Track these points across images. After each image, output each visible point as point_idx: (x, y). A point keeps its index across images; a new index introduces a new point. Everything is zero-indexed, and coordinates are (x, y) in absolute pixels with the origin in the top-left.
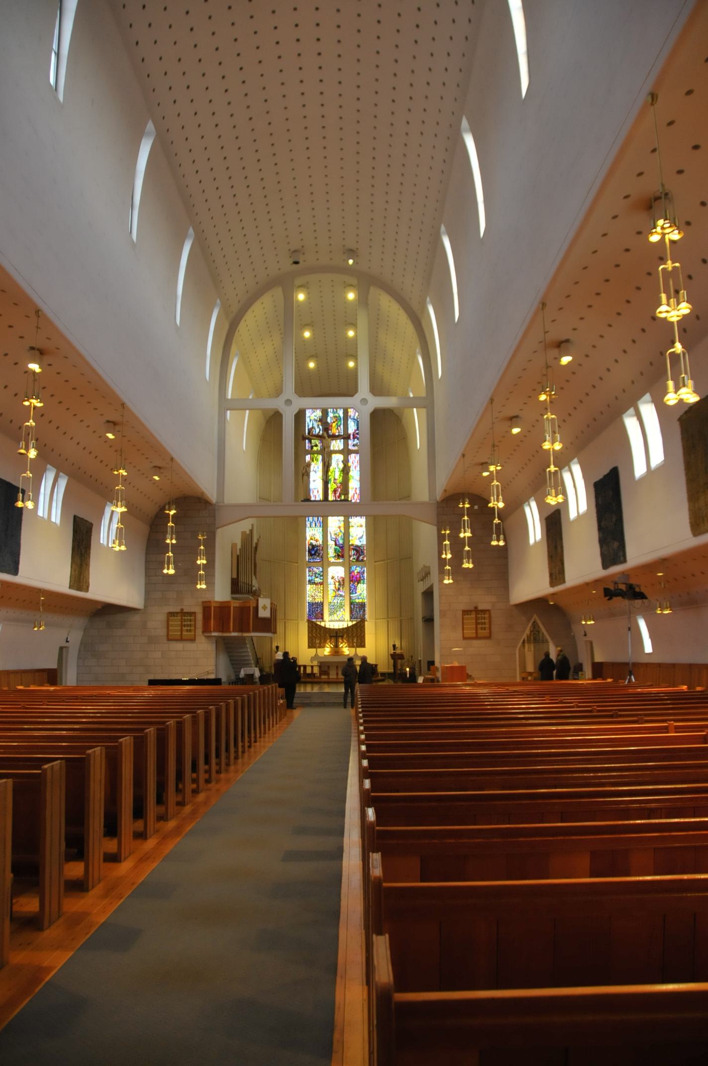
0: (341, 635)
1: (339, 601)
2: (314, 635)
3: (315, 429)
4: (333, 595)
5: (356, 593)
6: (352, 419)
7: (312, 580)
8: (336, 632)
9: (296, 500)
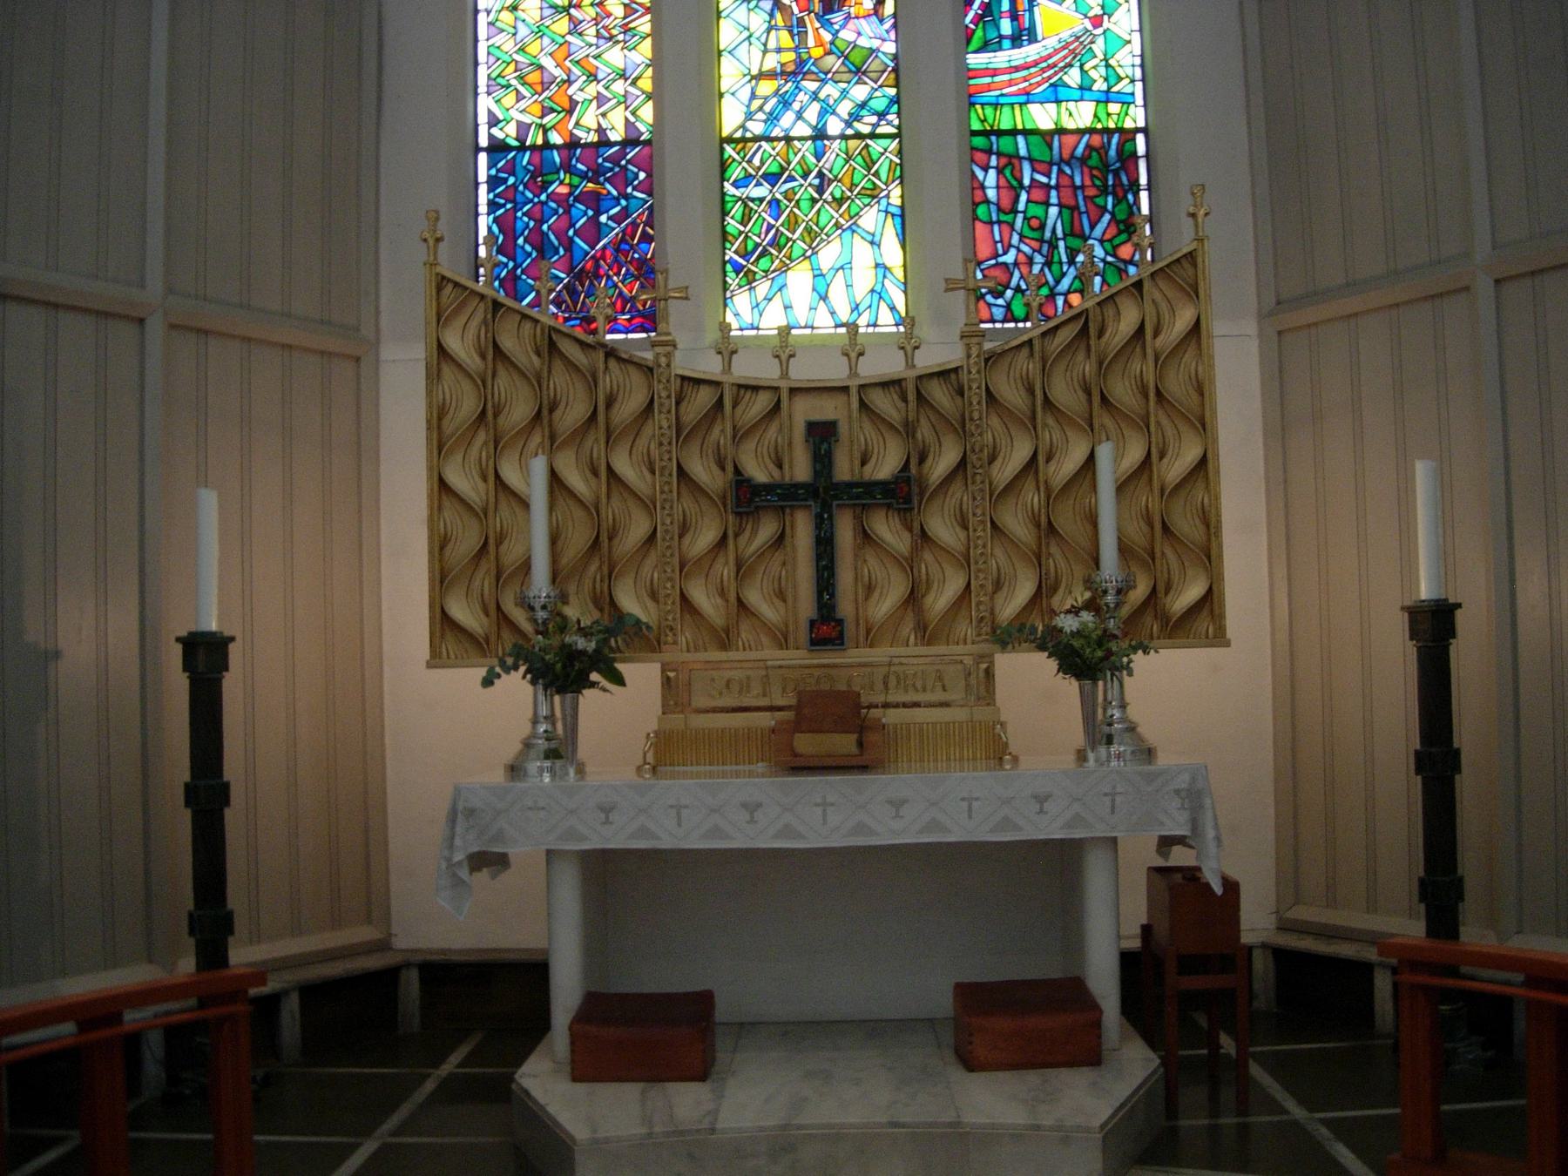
0: (885, 467)
1: (834, 127)
4: (771, 62)
5: (1024, 34)
8: (822, 434)
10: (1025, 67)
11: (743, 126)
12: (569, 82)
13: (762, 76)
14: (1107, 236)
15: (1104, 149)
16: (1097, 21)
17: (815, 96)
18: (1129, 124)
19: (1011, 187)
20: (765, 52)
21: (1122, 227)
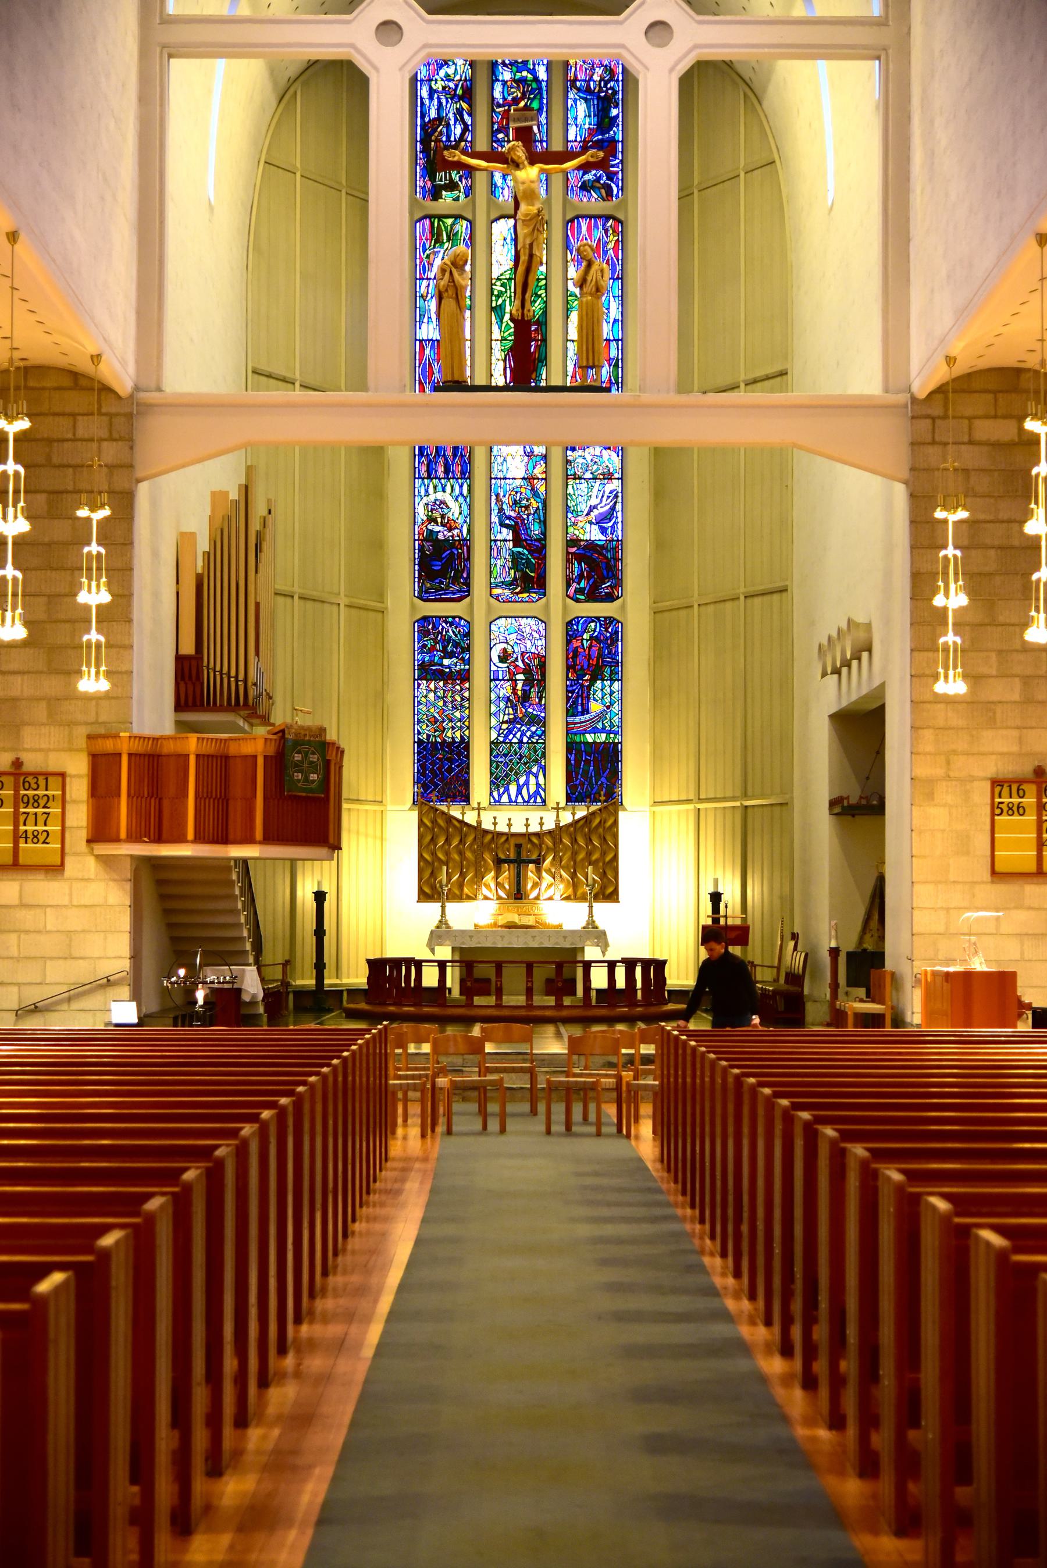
0: (534, 857)
1: (525, 740)
2: (441, 855)
3: (448, 125)
5: (586, 711)
6: (579, 90)
7: (432, 663)
8: (519, 847)
9: (683, 386)
10: (585, 722)
11: (497, 738)
12: (443, 722)
13: (503, 722)
16: (608, 707)
17: (519, 730)
18: (616, 741)
20: (504, 715)
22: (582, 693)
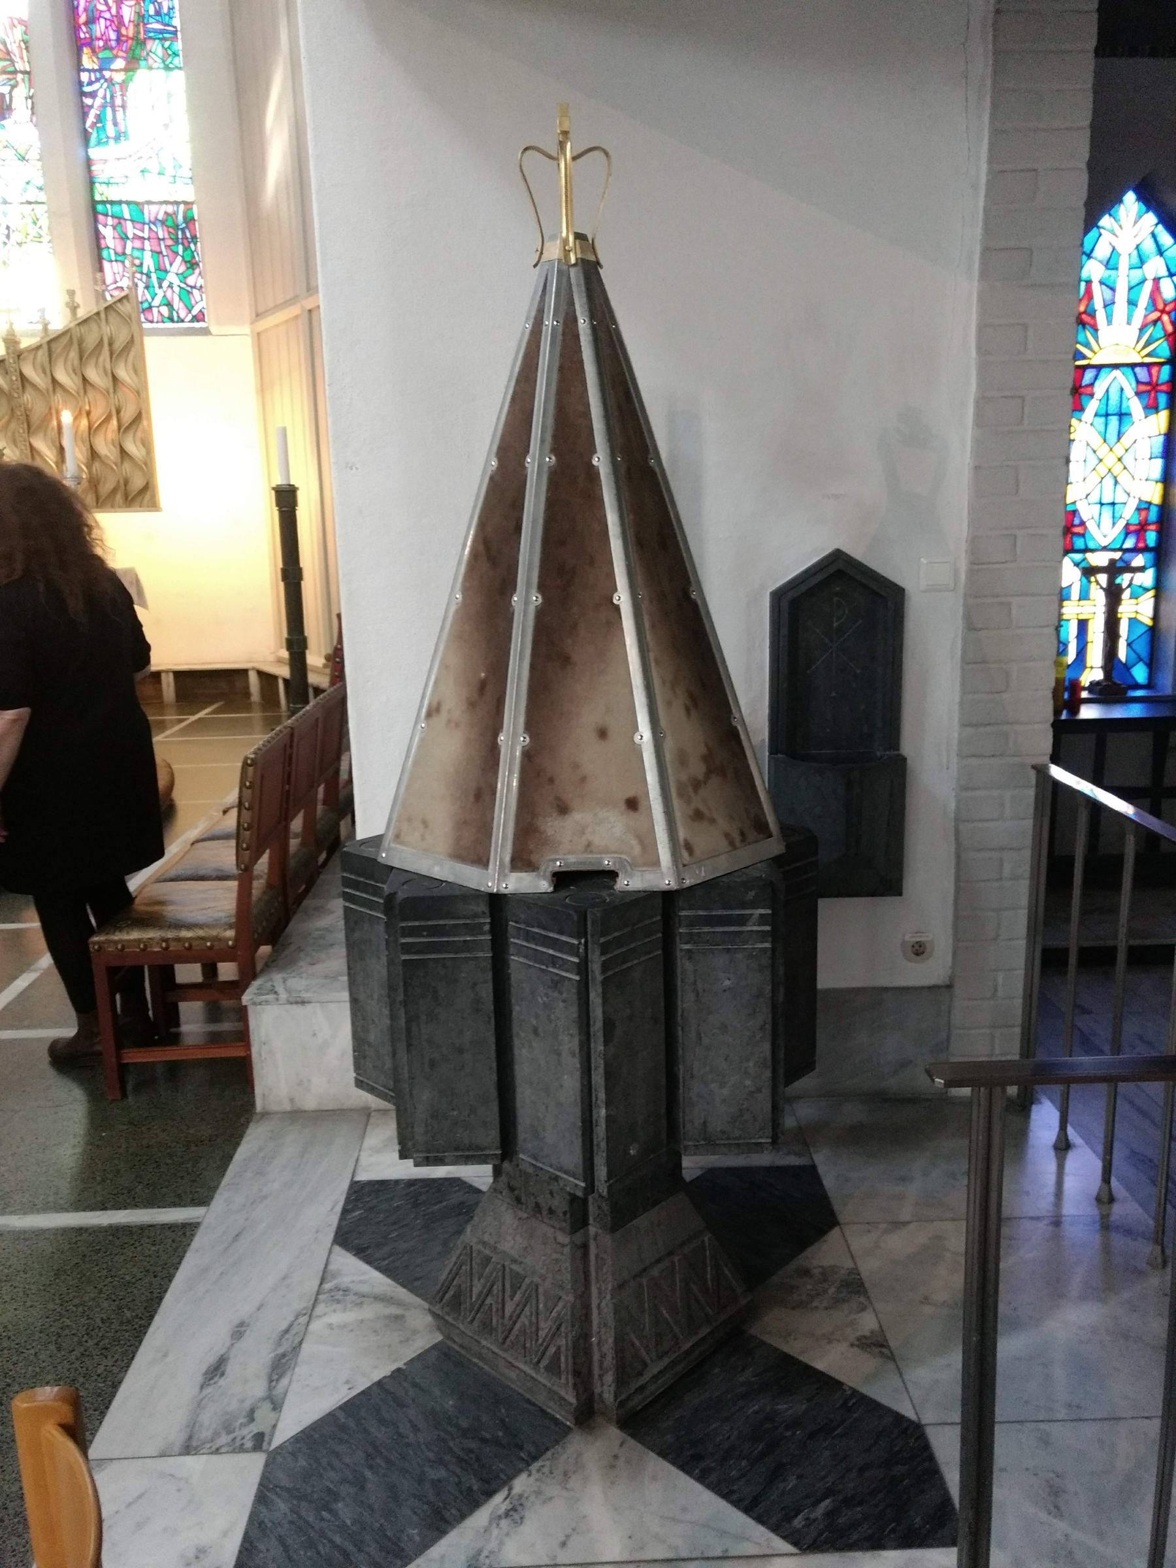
14: (180, 271)
15: (175, 214)
19: (122, 238)
21: (188, 265)
22: (112, 97)
